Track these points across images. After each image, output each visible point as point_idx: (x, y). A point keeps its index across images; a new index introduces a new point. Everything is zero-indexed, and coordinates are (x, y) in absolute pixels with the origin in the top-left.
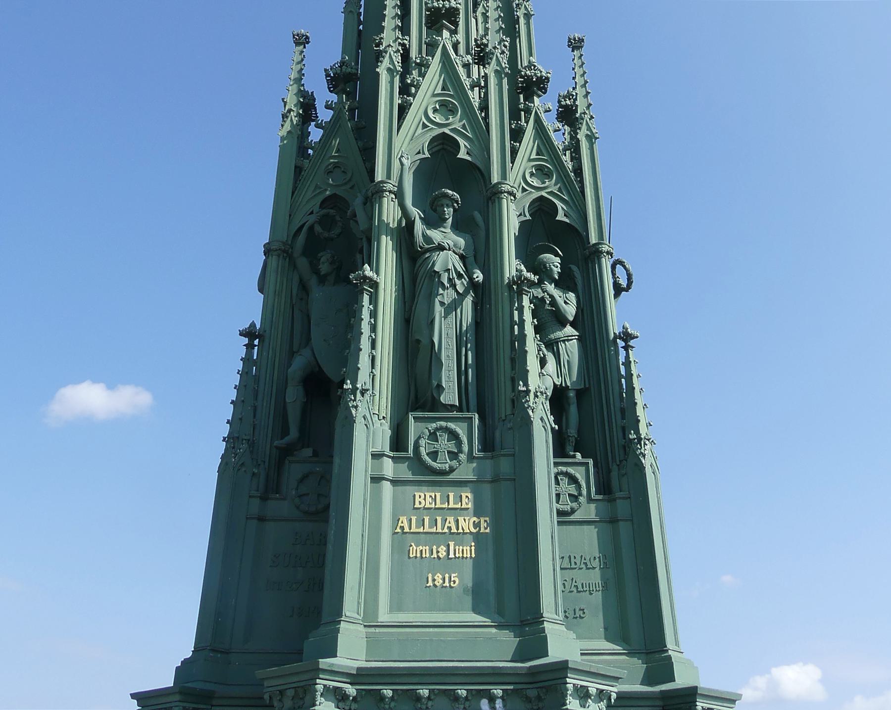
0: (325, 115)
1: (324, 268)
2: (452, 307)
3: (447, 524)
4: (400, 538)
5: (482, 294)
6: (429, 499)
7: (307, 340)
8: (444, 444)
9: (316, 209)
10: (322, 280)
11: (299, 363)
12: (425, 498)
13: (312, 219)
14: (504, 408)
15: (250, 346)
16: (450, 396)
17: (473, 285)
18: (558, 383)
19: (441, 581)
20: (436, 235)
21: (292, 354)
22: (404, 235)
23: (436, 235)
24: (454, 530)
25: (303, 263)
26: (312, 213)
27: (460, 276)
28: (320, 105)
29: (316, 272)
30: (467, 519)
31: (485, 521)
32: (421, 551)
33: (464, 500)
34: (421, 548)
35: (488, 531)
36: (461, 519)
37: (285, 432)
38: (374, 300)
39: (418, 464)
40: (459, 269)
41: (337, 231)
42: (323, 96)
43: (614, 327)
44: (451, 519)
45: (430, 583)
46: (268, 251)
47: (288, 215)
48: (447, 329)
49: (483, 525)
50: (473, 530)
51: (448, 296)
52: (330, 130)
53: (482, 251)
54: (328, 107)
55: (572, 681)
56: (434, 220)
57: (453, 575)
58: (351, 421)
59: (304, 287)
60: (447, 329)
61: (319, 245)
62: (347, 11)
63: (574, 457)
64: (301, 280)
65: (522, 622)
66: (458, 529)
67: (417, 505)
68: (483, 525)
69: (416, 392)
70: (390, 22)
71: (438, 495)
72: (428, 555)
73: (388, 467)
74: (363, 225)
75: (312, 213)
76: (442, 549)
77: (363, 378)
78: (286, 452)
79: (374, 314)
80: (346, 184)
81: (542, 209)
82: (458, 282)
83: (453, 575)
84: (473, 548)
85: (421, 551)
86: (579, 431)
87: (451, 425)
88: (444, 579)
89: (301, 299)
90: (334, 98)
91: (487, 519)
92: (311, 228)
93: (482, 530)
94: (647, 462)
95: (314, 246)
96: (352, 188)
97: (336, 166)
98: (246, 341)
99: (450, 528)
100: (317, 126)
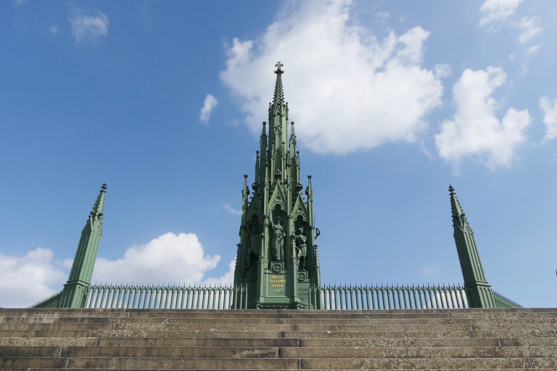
0: (252, 195)
1: (253, 231)
2: (280, 241)
4: (270, 283)
5: (285, 238)
7: (250, 246)
8: (277, 266)
10: (253, 234)
11: (249, 251)
12: (274, 276)
13: (251, 220)
14: (289, 260)
15: (239, 248)
16: (279, 258)
17: (283, 236)
20: (276, 226)
21: (247, 249)
22: (270, 226)
23: (276, 226)
25: (249, 230)
28: (251, 192)
29: (252, 232)
37: (246, 265)
38: (264, 240)
39: (273, 270)
42: (252, 190)
43: (314, 244)
46: (241, 227)
48: (279, 245)
51: (278, 239)
52: (253, 199)
53: (286, 229)
54: (253, 193)
55: (298, 305)
56: (276, 223)
58: (261, 263)
59: (249, 235)
60: (279, 245)
61: (252, 226)
62: (256, 168)
69: (272, 258)
70: (266, 178)
73: (267, 271)
74: (262, 224)
77: (262, 255)
78: (247, 269)
79: (264, 243)
81: (300, 218)
90: (254, 191)
94: (318, 271)
95: (251, 226)
97: (255, 208)
100: (251, 198)
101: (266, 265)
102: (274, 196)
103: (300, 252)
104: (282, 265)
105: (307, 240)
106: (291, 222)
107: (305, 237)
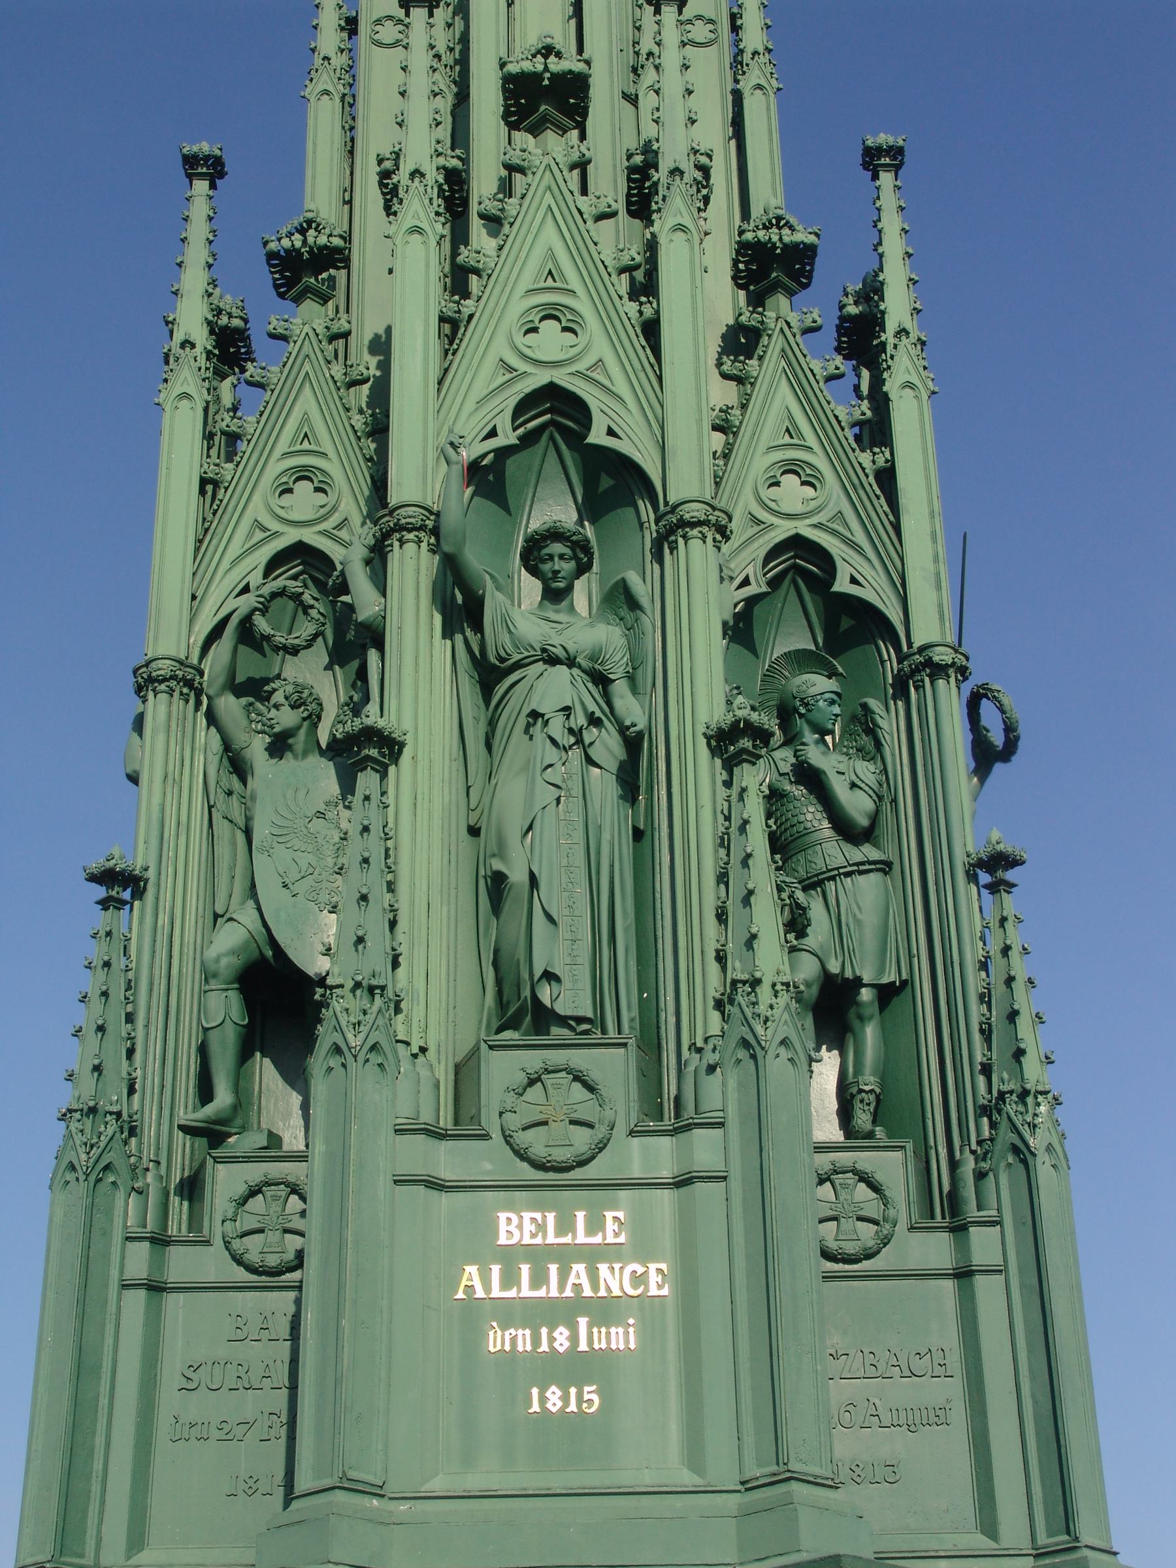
3: (572, 1280)
6: (529, 1227)
9: (256, 579)
13: (248, 602)
18: (834, 967)
19: (560, 1404)
24: (587, 1292)
26: (246, 590)
27: (594, 721)
30: (617, 1266)
31: (659, 1271)
32: (514, 1340)
33: (610, 1226)
34: (512, 1331)
35: (665, 1291)
36: (603, 1268)
40: (592, 707)
41: (305, 629)
44: (579, 1268)
45: (536, 1407)
47: (188, 597)
49: (654, 1278)
50: (631, 1291)
57: (587, 1389)
63: (870, 1135)
64: (227, 746)
65: (742, 1483)
66: (595, 1286)
67: (503, 1240)
68: (654, 1278)
71: (551, 1217)
72: (529, 1348)
75: (246, 590)
76: (562, 1338)
80: (324, 518)
82: (590, 735)
83: (587, 1389)
84: (631, 1330)
85: (514, 1340)
86: (884, 1077)
87: (578, 1058)
88: (565, 1399)
89: (230, 793)
91: (664, 1266)
92: (246, 624)
93: (653, 1291)
96: (339, 527)
97: (304, 474)
98: (101, 892)
99: (578, 1287)
101: (422, 1090)
102: (501, 309)
103: (819, 932)
104: (613, 1067)
105: (884, 796)
106: (703, 588)
107: (867, 771)
